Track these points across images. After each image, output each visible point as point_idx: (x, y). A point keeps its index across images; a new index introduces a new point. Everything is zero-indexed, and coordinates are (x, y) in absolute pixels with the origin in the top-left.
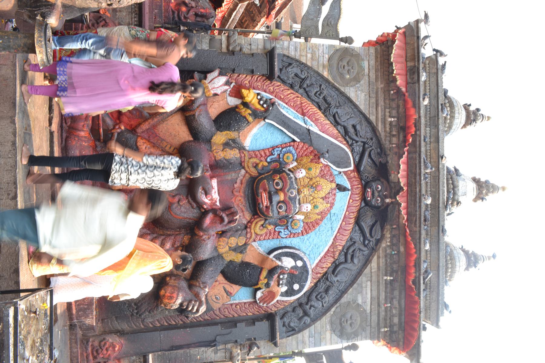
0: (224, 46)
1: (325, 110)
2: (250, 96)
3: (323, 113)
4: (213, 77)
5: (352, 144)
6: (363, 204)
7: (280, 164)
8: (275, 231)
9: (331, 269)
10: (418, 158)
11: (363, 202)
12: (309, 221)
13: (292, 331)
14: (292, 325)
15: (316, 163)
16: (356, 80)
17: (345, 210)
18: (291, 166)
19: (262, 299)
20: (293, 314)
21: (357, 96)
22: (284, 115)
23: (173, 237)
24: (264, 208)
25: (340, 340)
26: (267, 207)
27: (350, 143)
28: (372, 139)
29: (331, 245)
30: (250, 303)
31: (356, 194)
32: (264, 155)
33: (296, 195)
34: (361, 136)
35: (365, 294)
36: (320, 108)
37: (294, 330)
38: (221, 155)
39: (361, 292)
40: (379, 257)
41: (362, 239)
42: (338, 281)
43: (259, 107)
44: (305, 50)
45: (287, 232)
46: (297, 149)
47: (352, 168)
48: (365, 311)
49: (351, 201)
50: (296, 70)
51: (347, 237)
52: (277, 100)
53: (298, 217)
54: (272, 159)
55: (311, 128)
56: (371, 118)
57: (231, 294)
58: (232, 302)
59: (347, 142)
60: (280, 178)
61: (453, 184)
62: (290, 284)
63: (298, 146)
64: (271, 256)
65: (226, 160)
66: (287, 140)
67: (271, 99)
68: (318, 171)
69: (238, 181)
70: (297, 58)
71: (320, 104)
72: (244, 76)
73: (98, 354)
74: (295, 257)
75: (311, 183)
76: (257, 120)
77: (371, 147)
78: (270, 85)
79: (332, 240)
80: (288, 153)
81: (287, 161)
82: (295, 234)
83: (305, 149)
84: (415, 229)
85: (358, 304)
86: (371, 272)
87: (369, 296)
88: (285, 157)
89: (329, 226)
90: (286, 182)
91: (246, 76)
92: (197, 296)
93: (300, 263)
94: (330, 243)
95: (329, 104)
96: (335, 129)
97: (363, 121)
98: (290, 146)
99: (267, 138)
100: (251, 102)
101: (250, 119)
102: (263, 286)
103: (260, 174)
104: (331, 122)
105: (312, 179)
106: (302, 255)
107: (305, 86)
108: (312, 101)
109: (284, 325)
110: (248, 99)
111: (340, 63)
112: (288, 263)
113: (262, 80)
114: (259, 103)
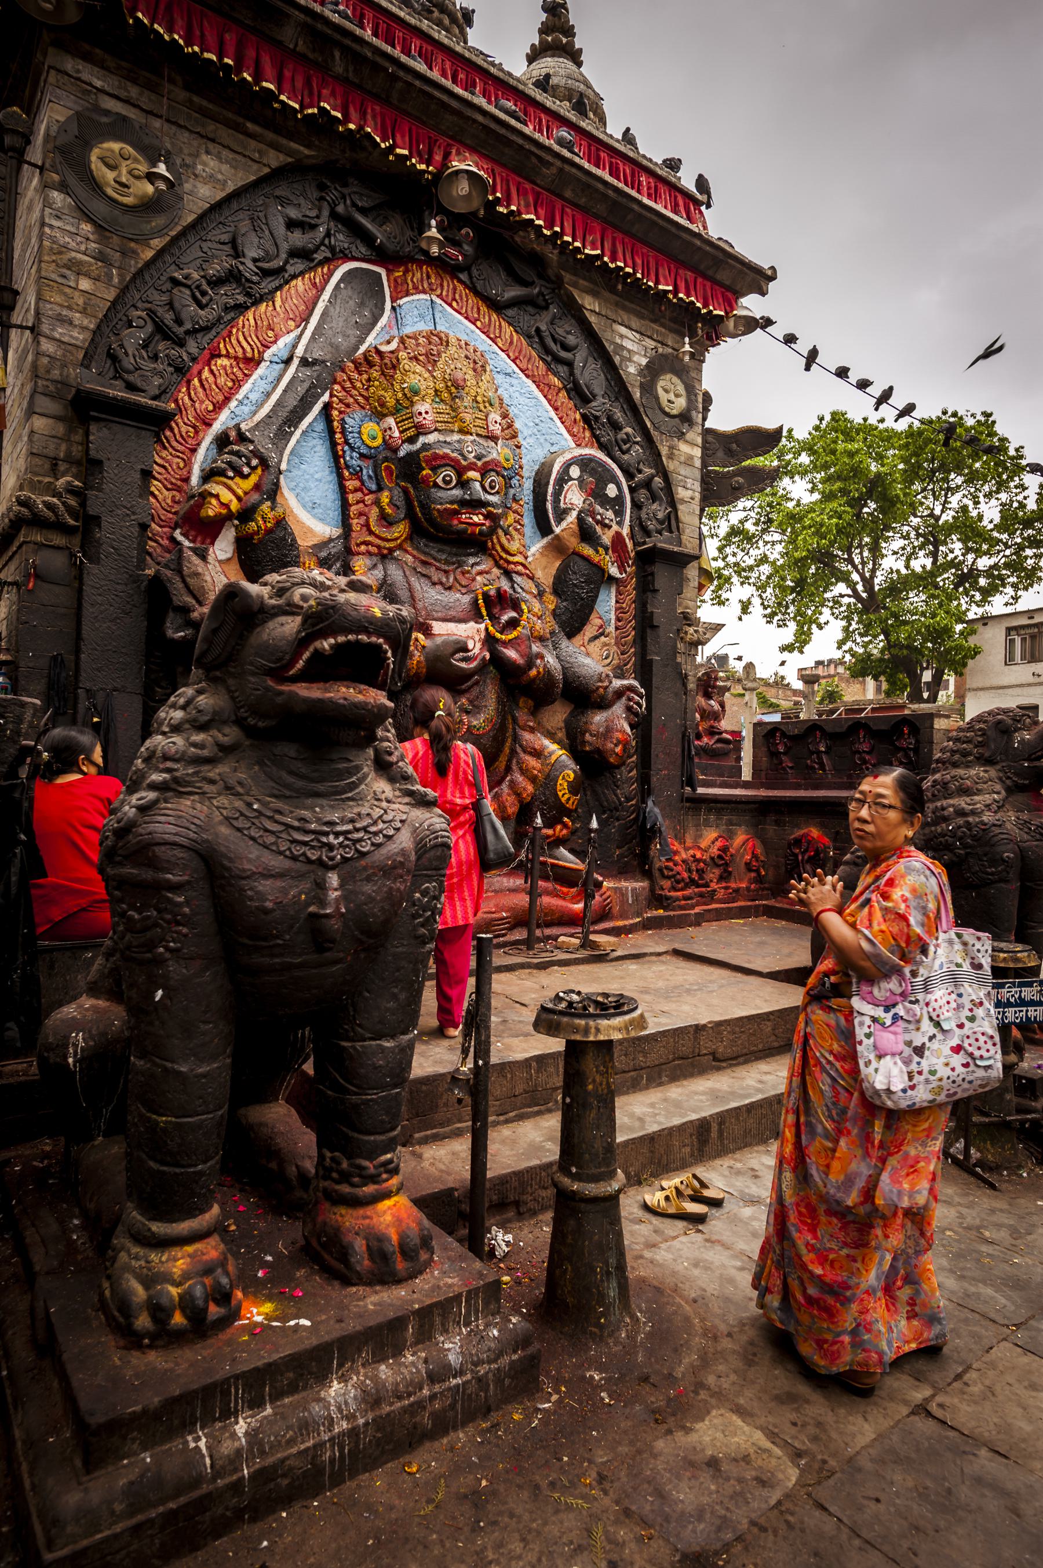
0: (59, 540)
1: (248, 295)
2: (226, 495)
3: (256, 303)
4: (183, 591)
5: (332, 249)
6: (463, 276)
7: (386, 459)
10: (409, 78)
11: (461, 276)
14: (660, 515)
15: (394, 367)
17: (473, 327)
18: (397, 434)
20: (645, 510)
22: (268, 416)
23: (518, 730)
24: (487, 523)
26: (486, 517)
27: (329, 255)
28: (322, 187)
29: (538, 386)
30: (619, 593)
31: (442, 286)
32: (359, 495)
34: (318, 217)
35: (633, 347)
36: (241, 309)
39: (629, 351)
40: (575, 285)
41: (530, 309)
43: (254, 479)
44: (68, 290)
45: (514, 481)
46: (348, 406)
47: (383, 272)
49: (454, 304)
50: (133, 339)
52: (217, 427)
54: (370, 477)
55: (300, 351)
56: (274, 164)
57: (601, 627)
59: (326, 261)
60: (434, 469)
63: (341, 401)
64: (557, 530)
66: (320, 426)
67: (222, 441)
68: (419, 369)
70: (92, 326)
71: (232, 302)
72: (152, 499)
73: (683, 880)
74: (564, 478)
75: (445, 395)
77: (344, 197)
78: (176, 431)
79: (529, 382)
80: (359, 433)
81: (379, 441)
83: (348, 385)
84: (554, 170)
85: (647, 366)
86: (598, 314)
88: (368, 442)
90: (446, 456)
91: (153, 494)
92: (619, 694)
93: (575, 472)
94: (533, 387)
95: (233, 276)
96: (294, 282)
97: (278, 192)
98: (343, 422)
99: (312, 476)
100: (239, 499)
103: (410, 515)
104: (279, 288)
105: (436, 391)
109: (660, 532)
110: (235, 506)
111: (110, 191)
112: (574, 497)
113: (164, 453)
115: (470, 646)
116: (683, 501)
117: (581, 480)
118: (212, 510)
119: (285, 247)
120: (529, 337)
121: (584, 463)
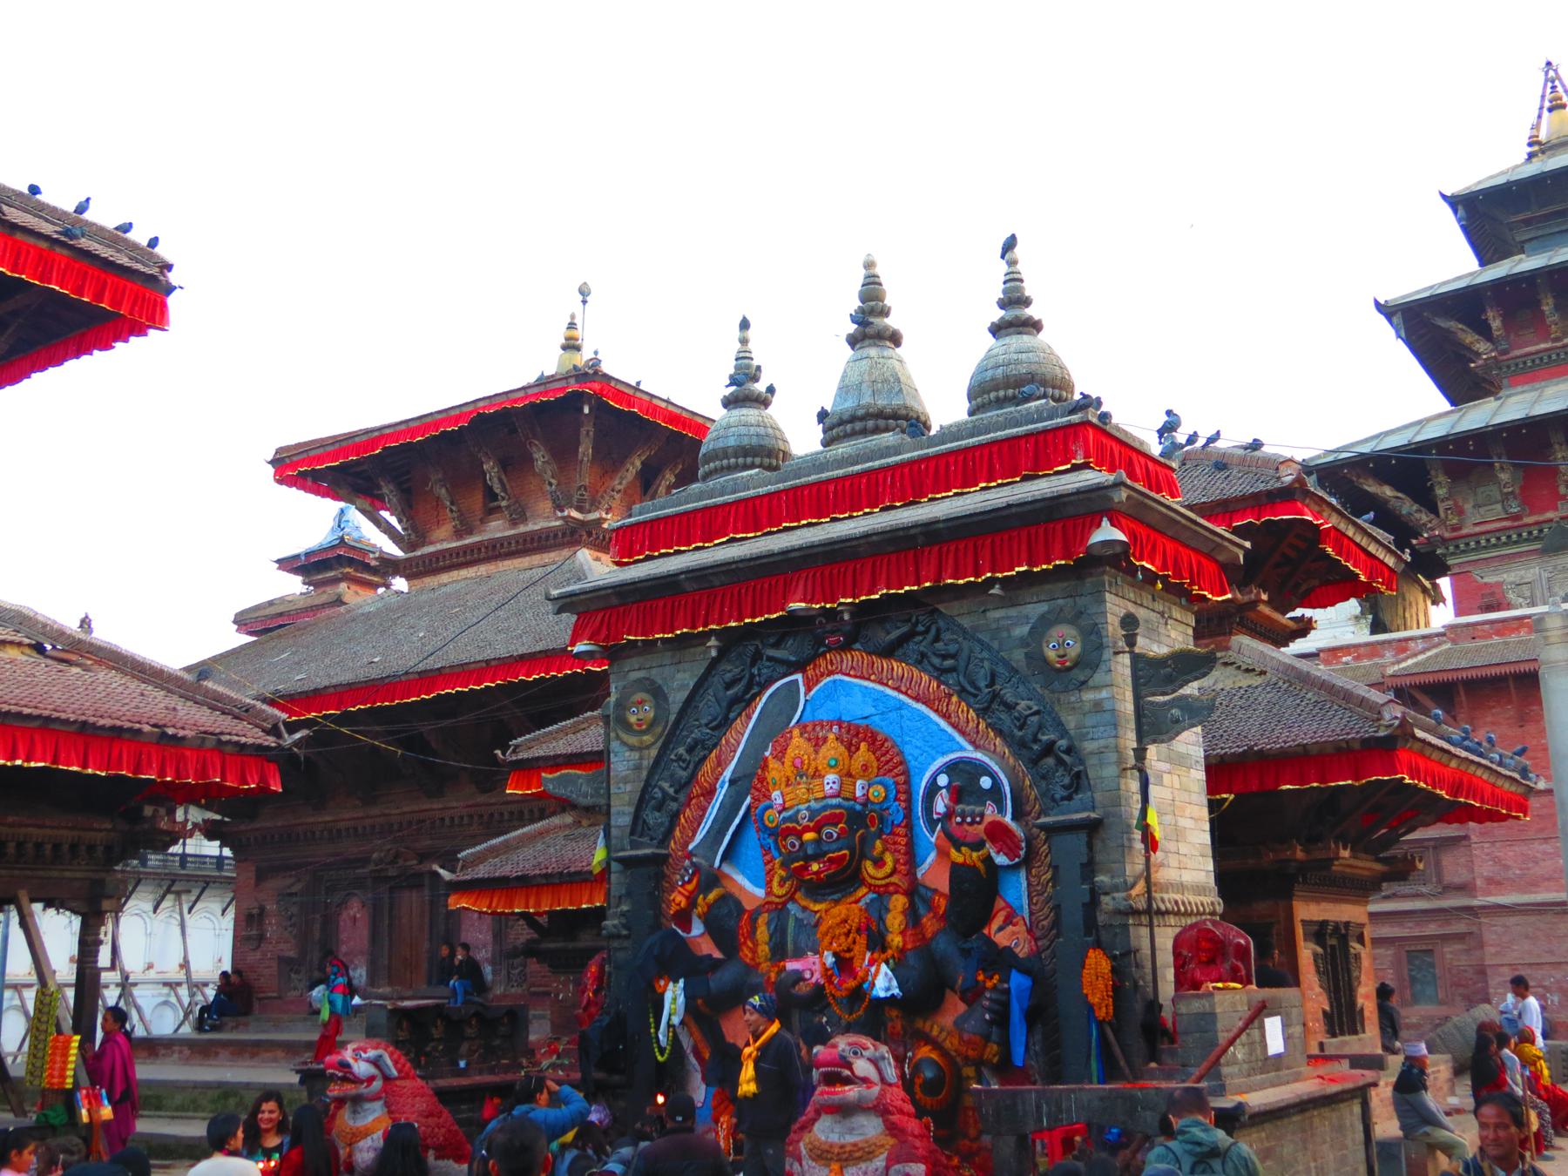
0: (626, 944)
2: (679, 899)
5: (759, 684)
6: (857, 646)
8: (892, 833)
9: (972, 700)
12: (875, 764)
13: (1078, 781)
14: (1067, 781)
16: (658, 694)
17: (866, 683)
19: (1011, 853)
21: (682, 687)
25: (1103, 667)
33: (808, 809)
36: (704, 758)
37: (1078, 775)
38: (764, 949)
40: (942, 602)
42: (992, 684)
47: (799, 677)
48: (1042, 617)
51: (916, 672)
53: (859, 793)
58: (1027, 916)
61: (839, 425)
62: (982, 796)
65: (771, 937)
69: (800, 915)
70: (632, 809)
76: (725, 882)
82: (898, 792)
85: (1030, 633)
87: (1013, 612)
89: (893, 715)
93: (943, 780)
100: (687, 898)
101: (711, 896)
102: (975, 855)
106: (928, 775)
107: (671, 791)
108: (693, 775)
109: (1069, 798)
112: (940, 806)
114: (690, 882)
115: (807, 975)
116: (1091, 753)
117: (948, 787)
118: (674, 908)
119: (724, 704)
120: (920, 662)
121: (951, 768)
